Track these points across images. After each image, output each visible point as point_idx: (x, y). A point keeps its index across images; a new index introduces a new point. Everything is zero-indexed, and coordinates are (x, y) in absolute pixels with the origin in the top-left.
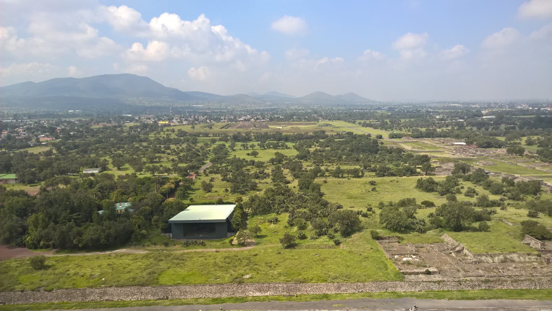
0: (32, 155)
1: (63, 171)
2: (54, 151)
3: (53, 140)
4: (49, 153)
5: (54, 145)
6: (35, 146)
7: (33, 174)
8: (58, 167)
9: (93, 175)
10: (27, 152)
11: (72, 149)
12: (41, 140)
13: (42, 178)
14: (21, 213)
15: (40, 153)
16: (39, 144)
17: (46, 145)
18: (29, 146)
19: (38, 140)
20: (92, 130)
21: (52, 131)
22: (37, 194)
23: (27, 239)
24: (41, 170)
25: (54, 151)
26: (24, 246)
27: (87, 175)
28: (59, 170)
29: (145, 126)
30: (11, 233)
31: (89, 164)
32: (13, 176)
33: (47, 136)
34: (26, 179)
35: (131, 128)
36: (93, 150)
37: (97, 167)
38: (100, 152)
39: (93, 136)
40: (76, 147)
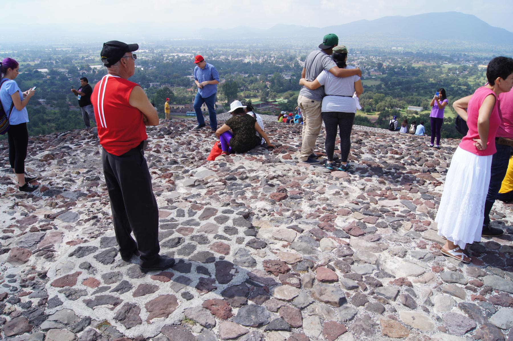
2: (383, 86)
5: (382, 80)
7: (370, 104)
8: (390, 101)
9: (416, 113)
11: (396, 85)
12: (371, 74)
13: (377, 109)
15: (372, 86)
17: (375, 79)
19: (369, 73)
20: (413, 68)
22: (375, 123)
24: (377, 102)
25: (383, 86)
27: (411, 112)
28: (390, 104)
29: (465, 68)
31: (414, 102)
35: (450, 69)
36: (414, 88)
37: (419, 106)
38: (422, 91)
39: (414, 74)
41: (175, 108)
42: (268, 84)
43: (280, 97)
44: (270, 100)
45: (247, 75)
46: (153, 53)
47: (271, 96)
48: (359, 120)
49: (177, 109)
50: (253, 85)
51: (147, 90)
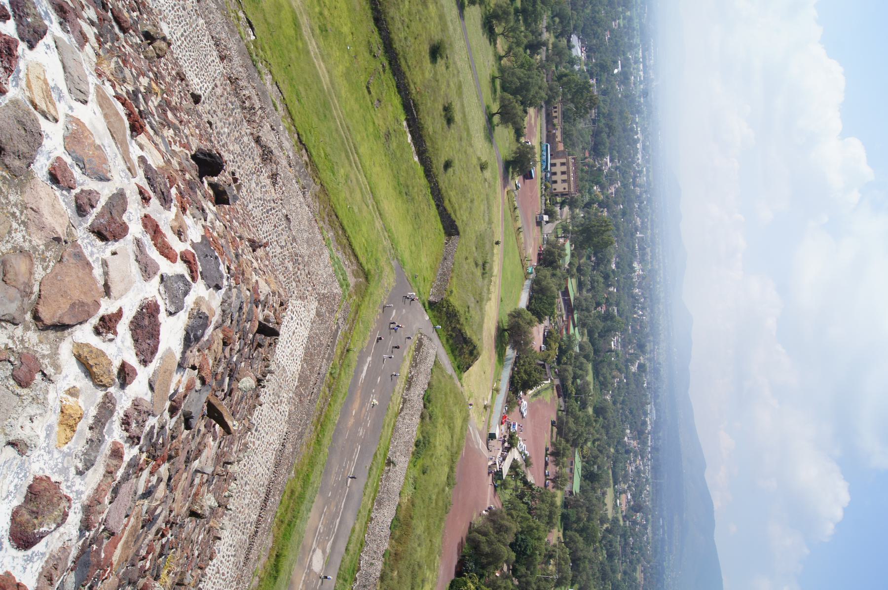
0: (604, 494)
1: (578, 565)
3: (622, 512)
4: (603, 520)
5: (615, 520)
6: (615, 491)
10: (607, 484)
11: (607, 550)
12: (623, 496)
14: (520, 546)
15: (606, 505)
16: (617, 494)
17: (615, 506)
18: (615, 483)
19: (625, 492)
21: (636, 507)
23: (470, 584)
24: (581, 531)
26: (459, 573)
30: (487, 555)
32: (576, 488)
33: (628, 502)
34: (571, 512)
40: (610, 556)
41: (555, 121)
42: (602, 310)
43: (582, 334)
44: (576, 316)
45: (613, 266)
46: (640, 97)
47: (583, 318)
48: (551, 512)
49: (554, 125)
50: (601, 280)
51: (584, 72)
